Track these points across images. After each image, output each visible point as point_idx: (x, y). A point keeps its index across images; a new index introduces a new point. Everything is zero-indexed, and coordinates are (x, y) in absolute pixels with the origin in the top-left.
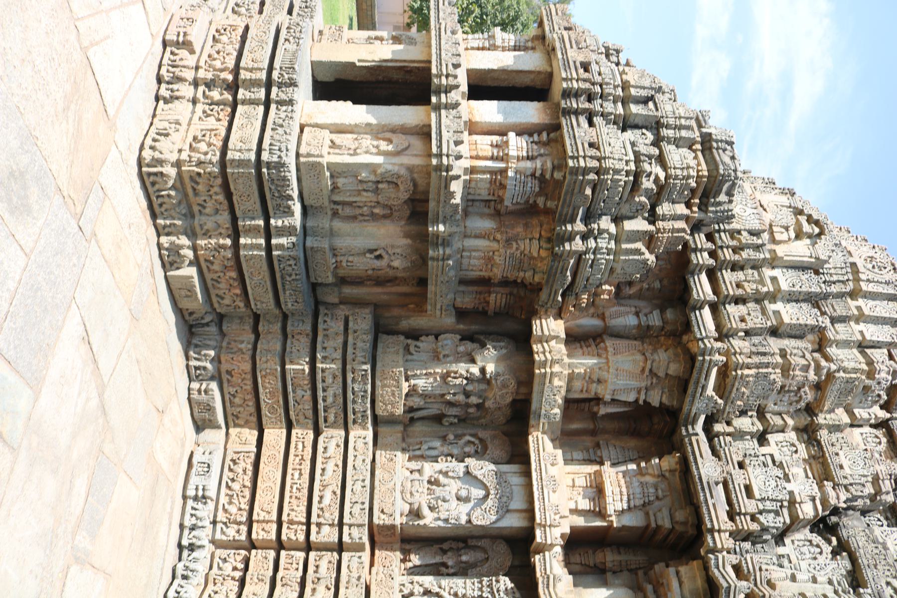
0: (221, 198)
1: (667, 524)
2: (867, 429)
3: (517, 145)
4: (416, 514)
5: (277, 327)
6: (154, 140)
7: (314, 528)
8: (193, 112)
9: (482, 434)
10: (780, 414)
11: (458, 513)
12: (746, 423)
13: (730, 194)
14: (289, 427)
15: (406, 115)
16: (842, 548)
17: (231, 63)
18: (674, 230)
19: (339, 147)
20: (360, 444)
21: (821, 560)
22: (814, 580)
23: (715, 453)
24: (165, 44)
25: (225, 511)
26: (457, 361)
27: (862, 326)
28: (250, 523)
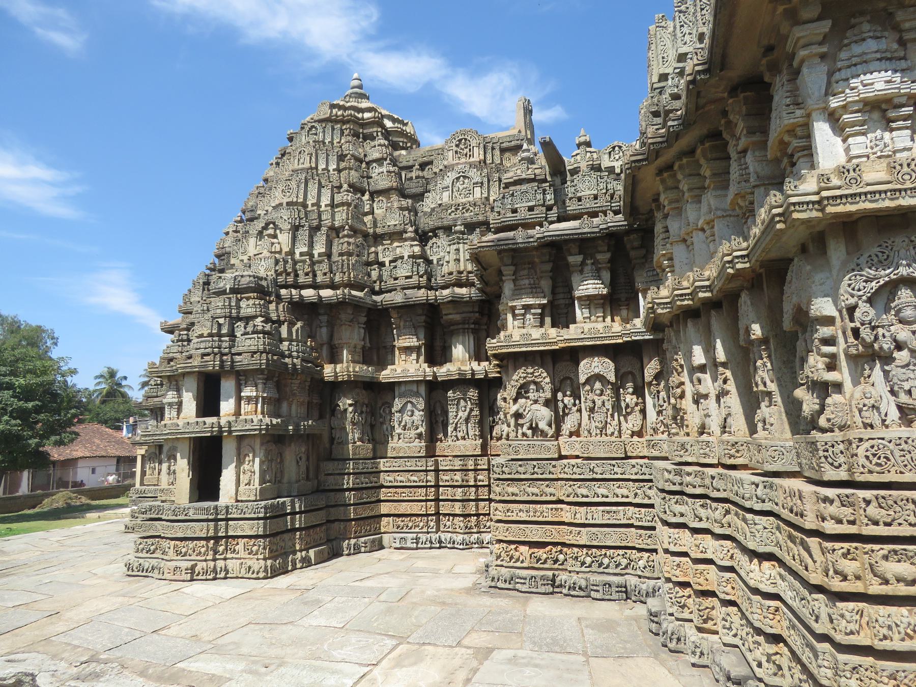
0: (278, 538)
1: (423, 318)
2: (375, 205)
3: (248, 392)
4: (420, 436)
5: (332, 510)
6: (253, 573)
7: (429, 484)
8: (232, 558)
9: (379, 404)
10: (369, 254)
11: (418, 416)
12: (374, 274)
13: (261, 279)
14: (380, 501)
15: (229, 449)
16: (435, 231)
17: (203, 543)
18: (284, 311)
19: (250, 481)
20: (388, 465)
21: (439, 244)
22: (449, 252)
23: (390, 291)
24: (192, 580)
25: (422, 528)
26: (346, 418)
27: (323, 204)
28: (427, 515)
